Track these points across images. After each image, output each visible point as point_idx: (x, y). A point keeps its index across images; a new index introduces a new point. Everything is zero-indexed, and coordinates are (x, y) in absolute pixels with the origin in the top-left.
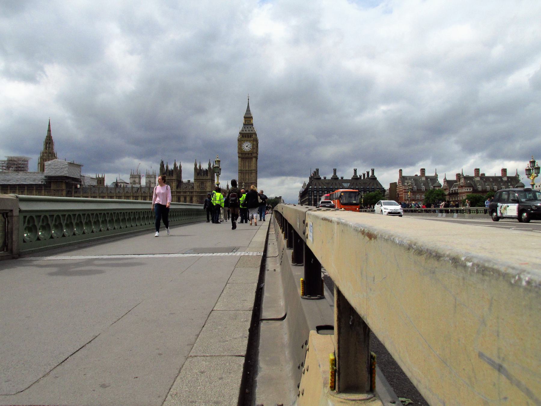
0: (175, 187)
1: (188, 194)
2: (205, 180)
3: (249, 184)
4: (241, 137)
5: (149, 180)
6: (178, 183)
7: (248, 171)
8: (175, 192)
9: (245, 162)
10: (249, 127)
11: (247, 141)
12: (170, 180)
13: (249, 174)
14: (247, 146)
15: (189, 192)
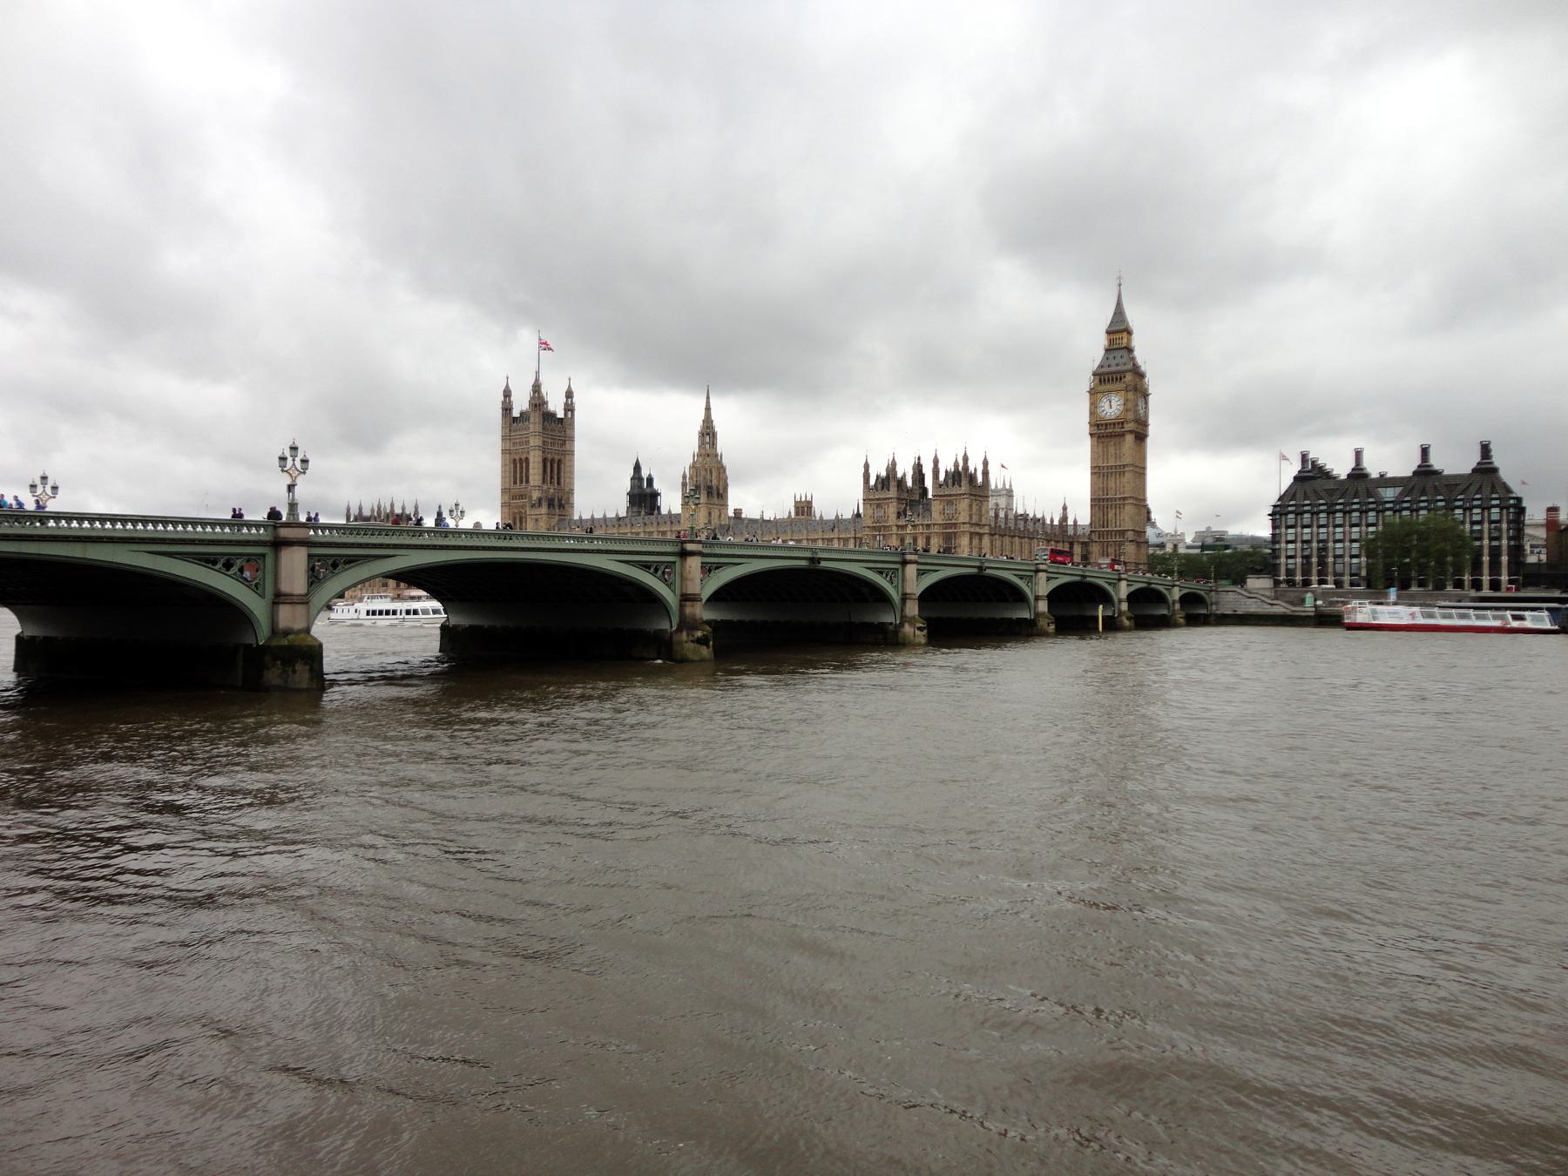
0: (895, 515)
1: (921, 531)
2: (956, 495)
3: (1118, 502)
4: (1097, 381)
5: (995, 501)
6: (904, 506)
7: (1116, 469)
8: (894, 528)
9: (1107, 448)
10: (1118, 354)
11: (1110, 391)
12: (885, 499)
13: (1118, 476)
14: (1112, 407)
15: (922, 525)
